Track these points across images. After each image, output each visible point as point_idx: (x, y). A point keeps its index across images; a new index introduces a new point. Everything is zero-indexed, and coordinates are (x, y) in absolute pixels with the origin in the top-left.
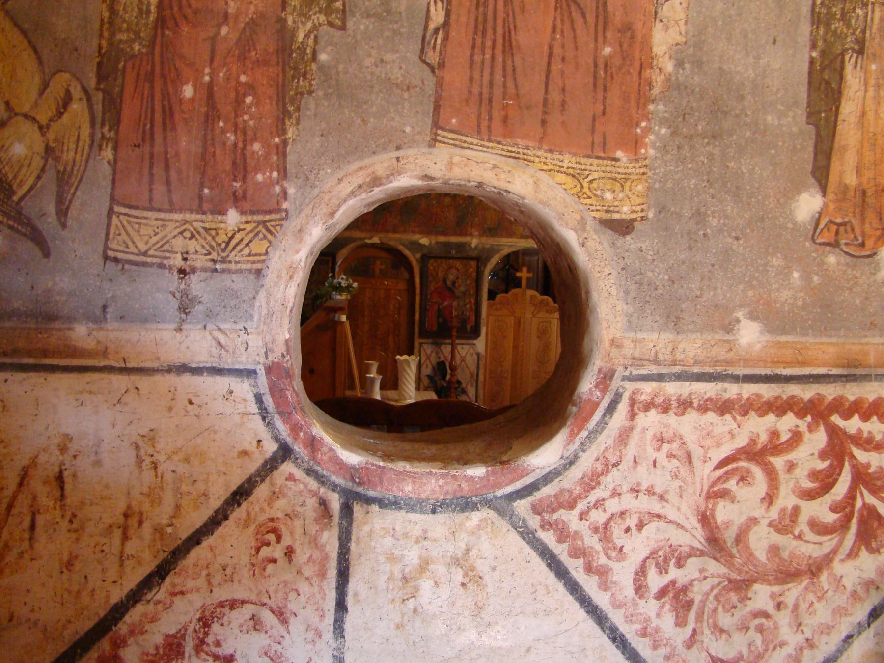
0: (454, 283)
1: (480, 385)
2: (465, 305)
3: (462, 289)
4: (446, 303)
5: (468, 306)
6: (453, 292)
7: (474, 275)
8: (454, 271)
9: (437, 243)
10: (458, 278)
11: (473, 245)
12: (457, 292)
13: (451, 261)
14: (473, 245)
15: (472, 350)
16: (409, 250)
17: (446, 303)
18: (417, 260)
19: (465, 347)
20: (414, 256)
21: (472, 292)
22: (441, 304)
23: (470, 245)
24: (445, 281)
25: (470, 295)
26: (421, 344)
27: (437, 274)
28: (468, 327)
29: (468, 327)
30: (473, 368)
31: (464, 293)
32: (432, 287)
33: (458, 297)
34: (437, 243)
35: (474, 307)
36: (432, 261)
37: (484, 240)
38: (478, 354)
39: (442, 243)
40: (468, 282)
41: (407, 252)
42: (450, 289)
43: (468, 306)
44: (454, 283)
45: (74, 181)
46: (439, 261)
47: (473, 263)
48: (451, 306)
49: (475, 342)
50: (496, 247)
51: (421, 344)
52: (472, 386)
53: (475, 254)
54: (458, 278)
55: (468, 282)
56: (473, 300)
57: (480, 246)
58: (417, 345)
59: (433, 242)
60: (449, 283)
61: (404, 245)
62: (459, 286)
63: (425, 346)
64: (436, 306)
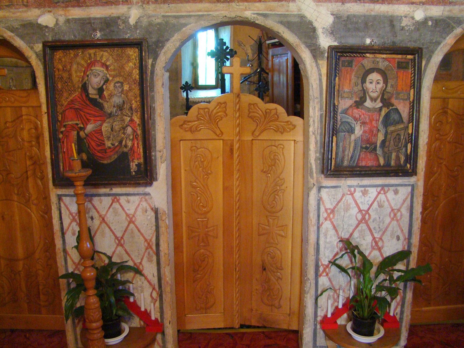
0: (100, 91)
1: (163, 260)
2: (124, 128)
3: (117, 100)
4: (90, 127)
5: (129, 130)
6: (101, 107)
7: (136, 74)
8: (98, 68)
9: (68, 21)
10: (107, 81)
11: (132, 21)
12: (108, 107)
13: (92, 51)
14: (132, 21)
15: (144, 204)
16: (22, 37)
17: (90, 127)
18: (37, 55)
19: (131, 198)
20: (32, 48)
21: (135, 104)
22: (83, 129)
23: (125, 21)
24: (85, 88)
25: (131, 108)
26: (60, 198)
27: (70, 75)
28: (133, 166)
29: (133, 166)
30: (150, 233)
31: (120, 108)
32: (64, 101)
33: (110, 115)
34: (68, 21)
35: (139, 132)
36: (59, 54)
37: (151, 9)
38: (156, 211)
39: (75, 20)
40: (126, 87)
41: (19, 43)
42: (94, 102)
43: (129, 130)
44: (100, 91)
45: (23, 23)
46: (72, 53)
47: (133, 53)
48: (99, 131)
49: (148, 190)
50: (173, 21)
51: (60, 198)
52: (150, 260)
53: (137, 35)
54: (107, 81)
55: (126, 87)
56: (137, 119)
57: (145, 21)
58: (54, 199)
59: (62, 20)
60: (92, 92)
61: (12, 30)
62: (111, 96)
63: (67, 200)
64: (75, 133)
